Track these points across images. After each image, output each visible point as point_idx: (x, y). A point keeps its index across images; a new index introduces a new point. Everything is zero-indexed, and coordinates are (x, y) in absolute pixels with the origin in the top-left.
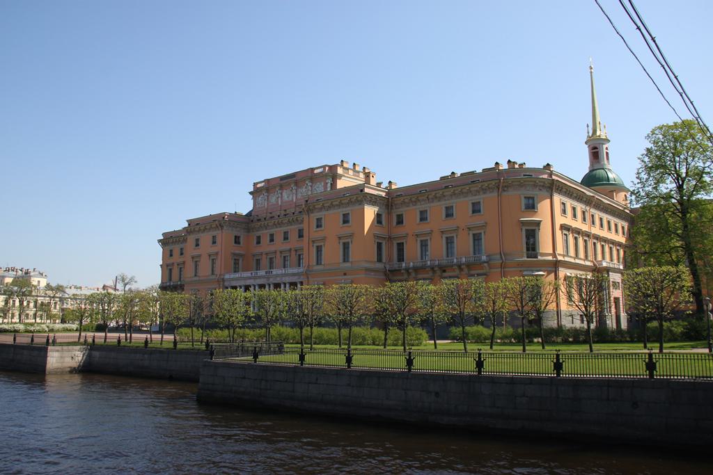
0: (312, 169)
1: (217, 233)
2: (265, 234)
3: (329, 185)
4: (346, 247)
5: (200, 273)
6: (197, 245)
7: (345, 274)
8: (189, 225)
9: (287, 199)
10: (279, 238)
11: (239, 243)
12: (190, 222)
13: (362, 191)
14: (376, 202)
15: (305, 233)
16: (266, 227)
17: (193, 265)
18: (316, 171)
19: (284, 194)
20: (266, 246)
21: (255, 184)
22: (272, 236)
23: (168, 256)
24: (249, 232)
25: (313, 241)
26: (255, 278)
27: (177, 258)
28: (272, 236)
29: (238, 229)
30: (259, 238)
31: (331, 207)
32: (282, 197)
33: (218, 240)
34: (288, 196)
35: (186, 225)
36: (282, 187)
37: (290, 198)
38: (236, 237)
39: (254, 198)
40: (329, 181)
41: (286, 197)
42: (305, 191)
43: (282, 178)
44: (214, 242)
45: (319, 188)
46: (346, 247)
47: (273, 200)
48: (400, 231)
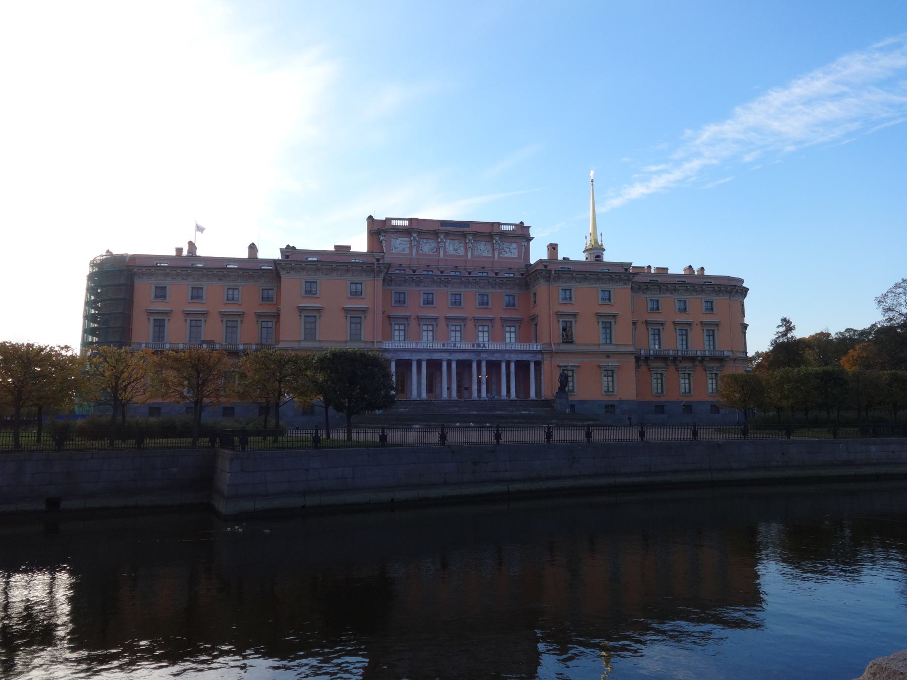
0: (499, 224)
4: (607, 327)
7: (608, 357)
8: (287, 257)
9: (453, 253)
12: (289, 252)
13: (626, 270)
16: (419, 283)
18: (503, 228)
19: (447, 244)
34: (452, 248)
35: (278, 256)
37: (461, 251)
41: (451, 248)
42: (483, 250)
45: (511, 251)
46: (607, 327)
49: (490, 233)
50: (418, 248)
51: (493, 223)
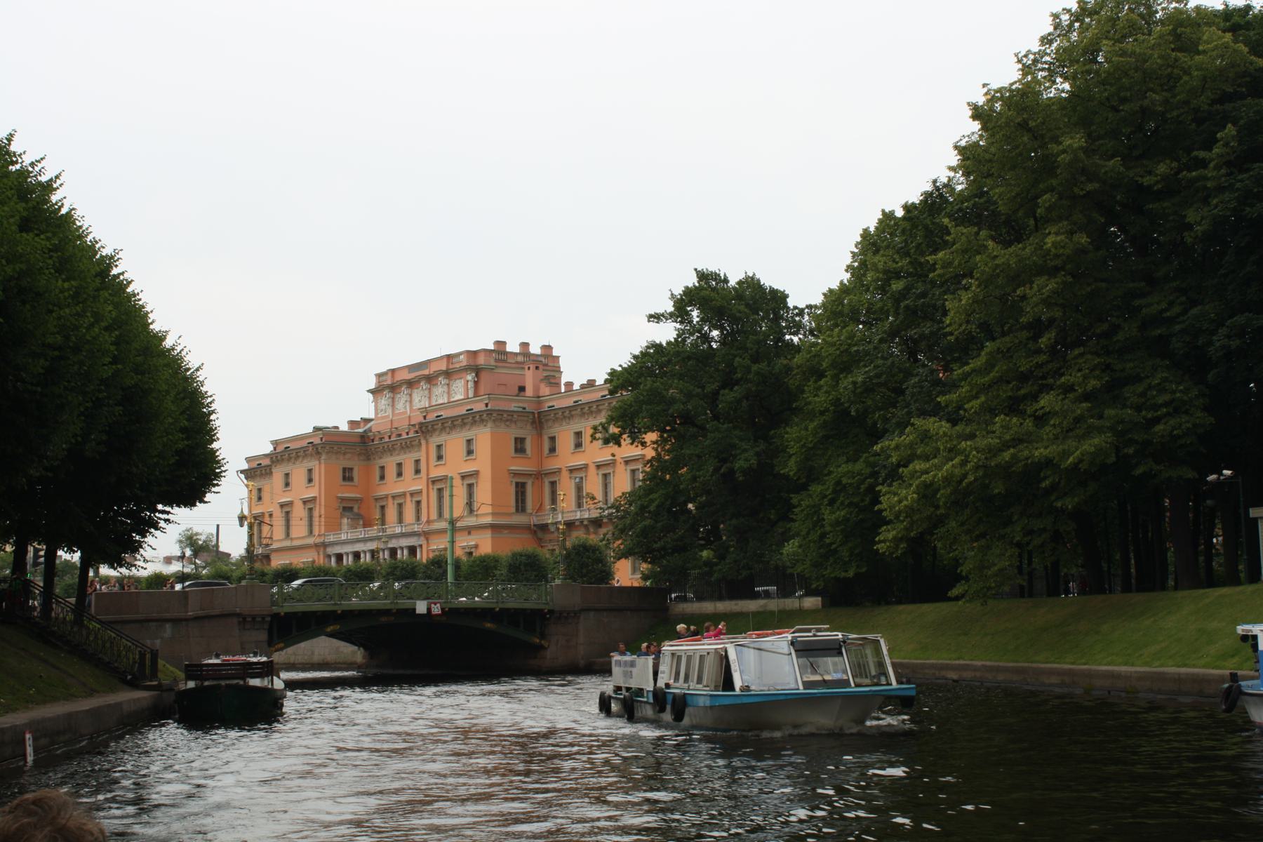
0: (449, 357)
1: (313, 464)
2: (390, 462)
3: (471, 385)
5: (294, 534)
6: (287, 484)
10: (409, 469)
11: (351, 479)
12: (276, 443)
14: (511, 421)
15: (423, 466)
17: (304, 514)
20: (393, 486)
21: (379, 376)
22: (400, 465)
23: (255, 498)
24: (369, 459)
25: (434, 482)
26: (365, 540)
27: (270, 505)
28: (400, 465)
29: (348, 456)
30: (382, 468)
31: (453, 427)
32: (411, 402)
33: (316, 476)
36: (411, 384)
38: (344, 469)
39: (376, 401)
40: (469, 378)
43: (411, 368)
44: (310, 480)
47: (400, 406)
48: (553, 464)
49: (448, 369)
50: (393, 406)
51: (442, 358)
